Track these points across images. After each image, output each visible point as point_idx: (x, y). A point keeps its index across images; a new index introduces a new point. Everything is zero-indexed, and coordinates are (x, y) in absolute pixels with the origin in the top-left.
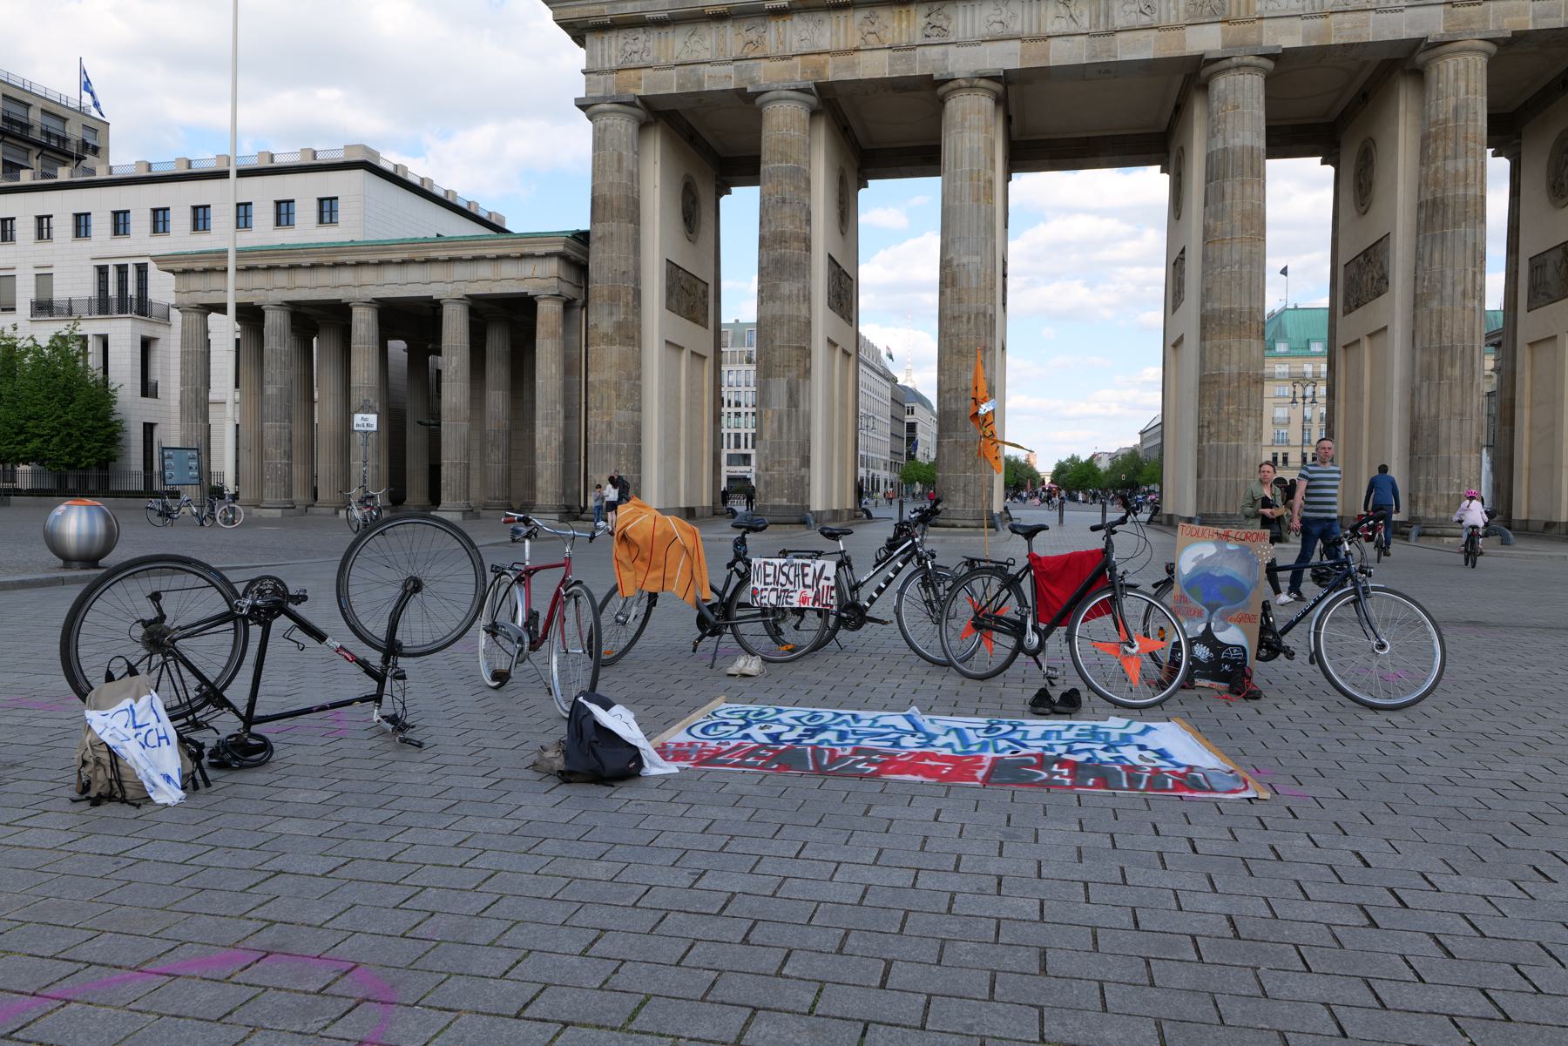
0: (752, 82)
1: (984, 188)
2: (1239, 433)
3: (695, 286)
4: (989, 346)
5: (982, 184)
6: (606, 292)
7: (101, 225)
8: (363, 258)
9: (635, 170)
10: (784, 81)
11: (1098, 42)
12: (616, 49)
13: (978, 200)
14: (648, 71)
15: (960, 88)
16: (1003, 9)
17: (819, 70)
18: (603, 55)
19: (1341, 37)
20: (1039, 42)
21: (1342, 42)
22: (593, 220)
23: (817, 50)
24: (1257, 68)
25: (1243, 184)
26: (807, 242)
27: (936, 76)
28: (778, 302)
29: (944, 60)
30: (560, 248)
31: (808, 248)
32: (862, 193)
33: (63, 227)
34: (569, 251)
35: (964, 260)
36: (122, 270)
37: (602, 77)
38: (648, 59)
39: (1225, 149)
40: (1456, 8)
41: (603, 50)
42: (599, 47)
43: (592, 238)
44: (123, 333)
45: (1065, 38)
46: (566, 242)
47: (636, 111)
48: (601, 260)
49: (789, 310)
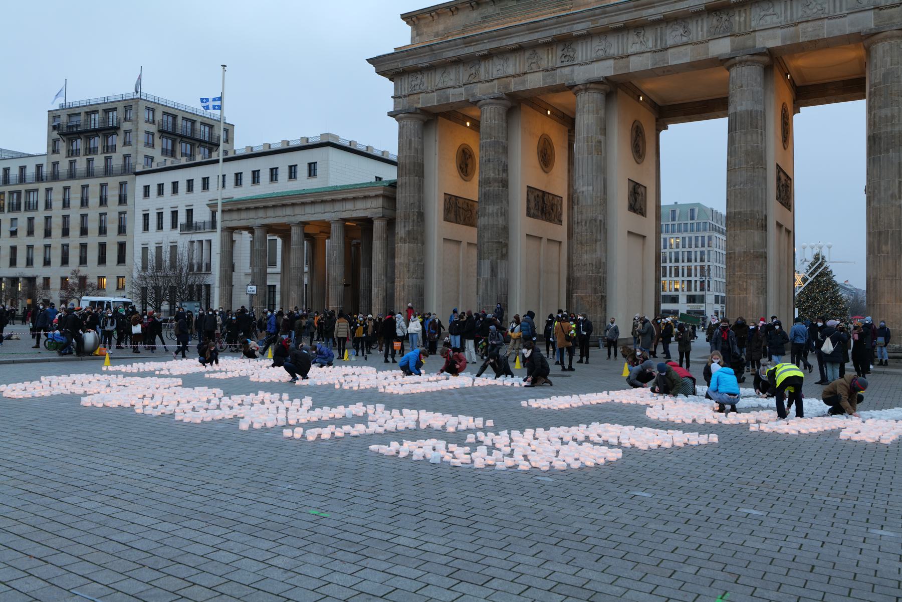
0: (473, 95)
1: (595, 146)
2: (746, 290)
3: (473, 205)
4: (599, 238)
5: (594, 144)
6: (403, 215)
8: (294, 201)
9: (419, 147)
10: (491, 94)
11: (658, 56)
12: (408, 84)
13: (591, 153)
14: (423, 95)
15: (580, 90)
16: (604, 42)
17: (507, 86)
18: (401, 88)
19: (806, 37)
20: (624, 59)
21: (806, 40)
22: (398, 176)
23: (505, 75)
24: (753, 63)
27: (566, 84)
28: (486, 218)
29: (572, 74)
30: (382, 192)
34: (387, 193)
35: (584, 189)
40: (882, 11)
41: (401, 85)
42: (400, 84)
43: (397, 186)
45: (638, 55)
46: (384, 188)
47: (418, 116)
49: (491, 221)
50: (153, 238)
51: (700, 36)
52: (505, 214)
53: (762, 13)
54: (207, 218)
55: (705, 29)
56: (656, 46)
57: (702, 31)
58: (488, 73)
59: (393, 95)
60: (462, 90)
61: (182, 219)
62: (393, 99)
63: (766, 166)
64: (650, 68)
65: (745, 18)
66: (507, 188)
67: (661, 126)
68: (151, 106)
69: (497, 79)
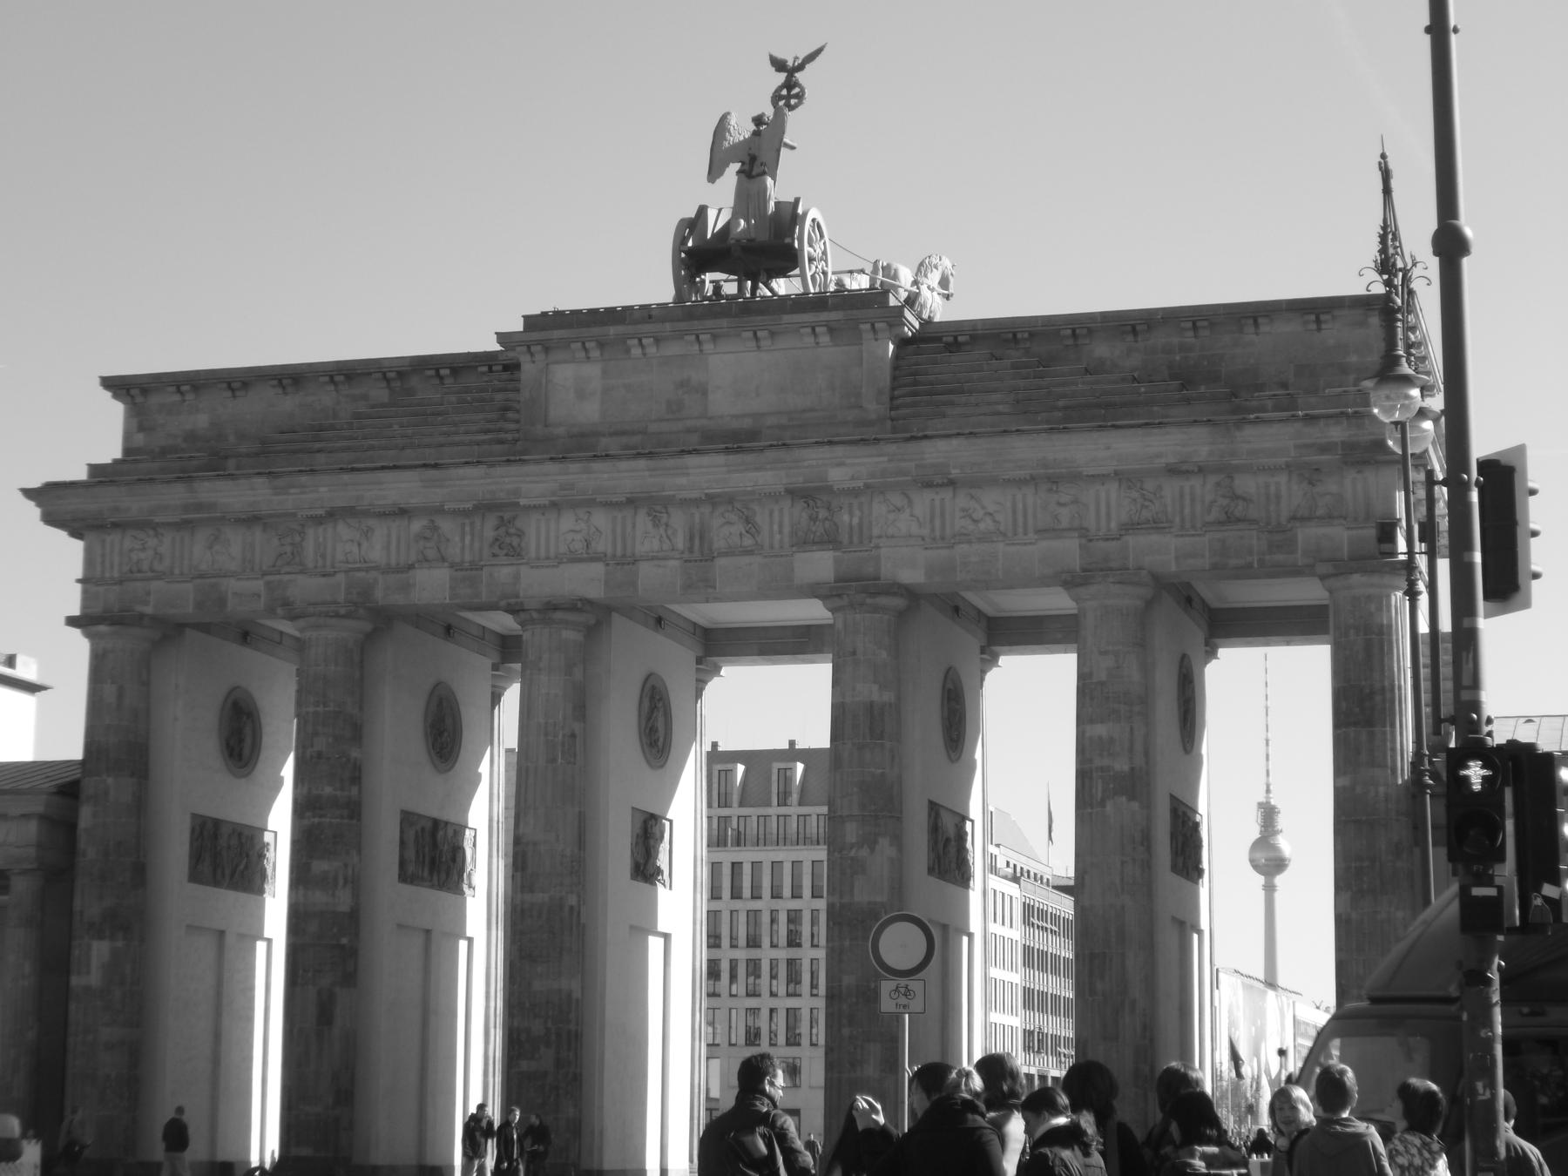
1: (563, 744)
13: (554, 760)
18: (103, 562)
37: (101, 589)
39: (843, 702)
51: (777, 545)
52: (355, 883)
53: (891, 516)
55: (786, 530)
56: (691, 550)
57: (780, 532)
58: (323, 556)
59: (80, 575)
60: (258, 585)
62: (79, 587)
63: (901, 812)
65: (861, 519)
66: (359, 820)
67: (705, 668)
69: (346, 572)
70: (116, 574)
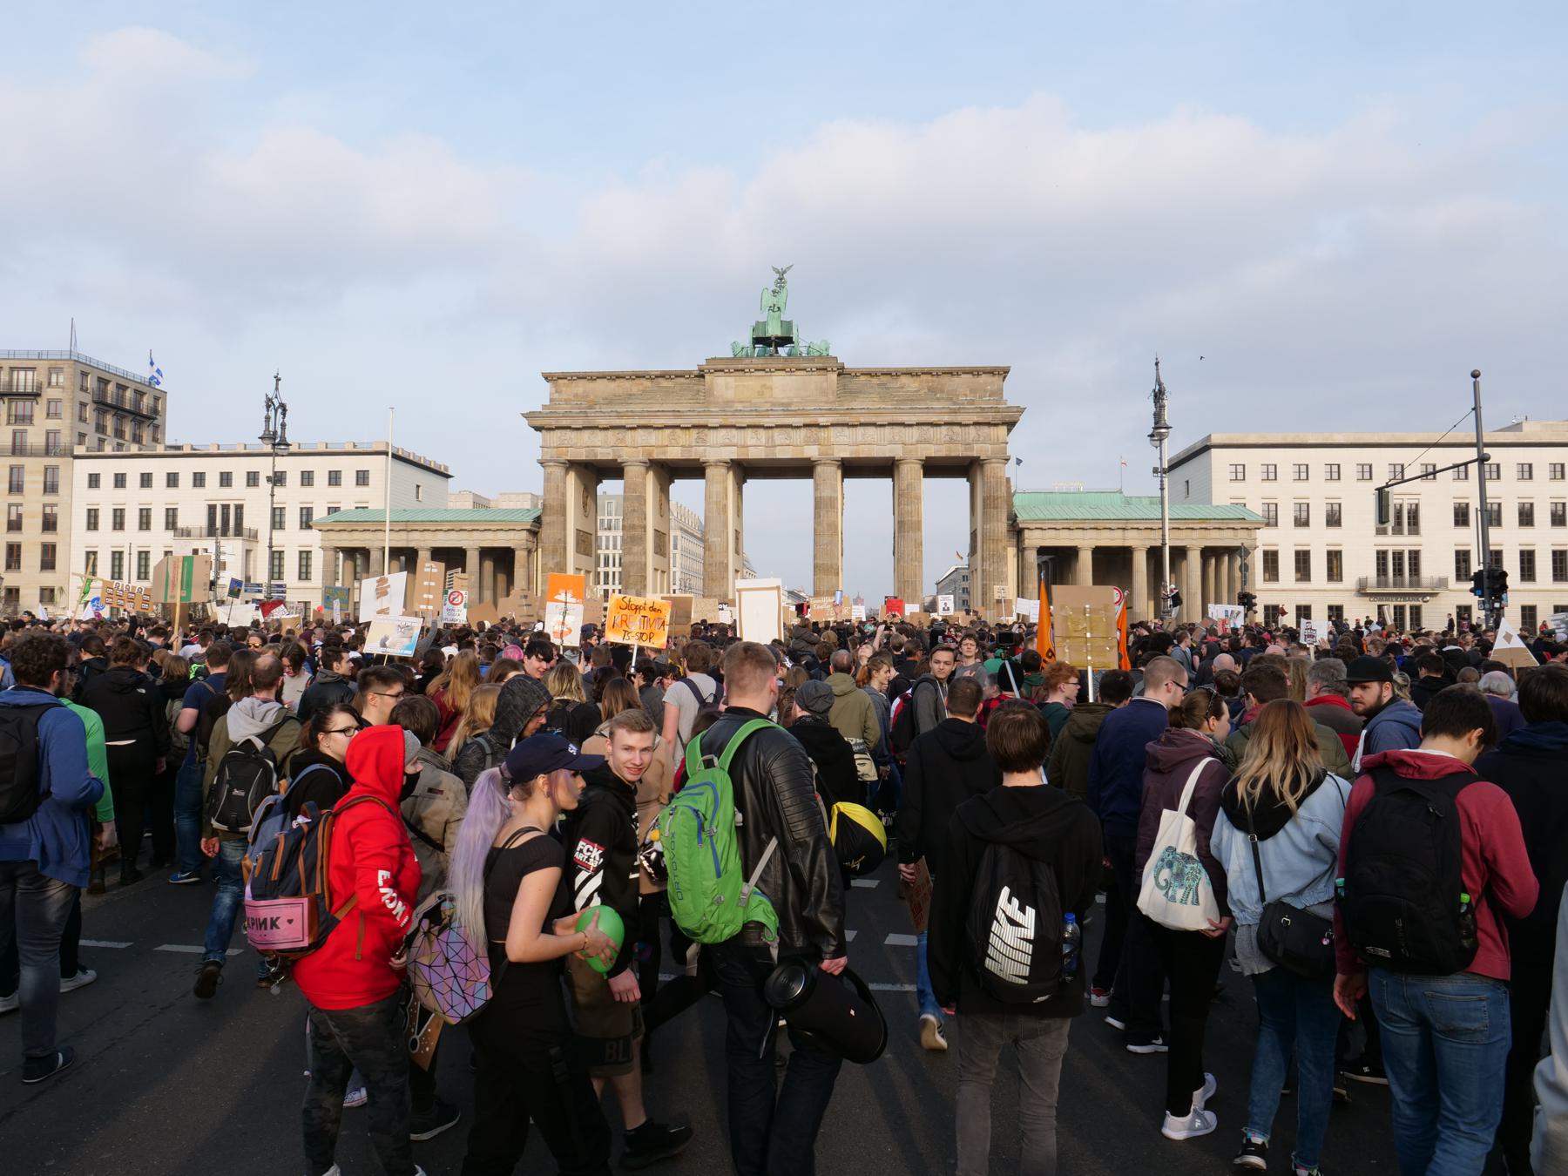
0: (620, 456)
6: (551, 548)
7: (212, 480)
13: (719, 514)
17: (650, 454)
25: (827, 511)
26: (644, 528)
27: (701, 460)
30: (529, 527)
31: (645, 531)
32: (672, 487)
33: (186, 480)
35: (715, 539)
36: (226, 508)
37: (549, 450)
38: (572, 443)
43: (544, 523)
44: (232, 548)
48: (546, 532)
49: (637, 559)
50: (105, 540)
54: (203, 521)
59: (540, 443)
60: (610, 450)
61: (158, 519)
64: (763, 457)
68: (87, 369)
70: (555, 445)
